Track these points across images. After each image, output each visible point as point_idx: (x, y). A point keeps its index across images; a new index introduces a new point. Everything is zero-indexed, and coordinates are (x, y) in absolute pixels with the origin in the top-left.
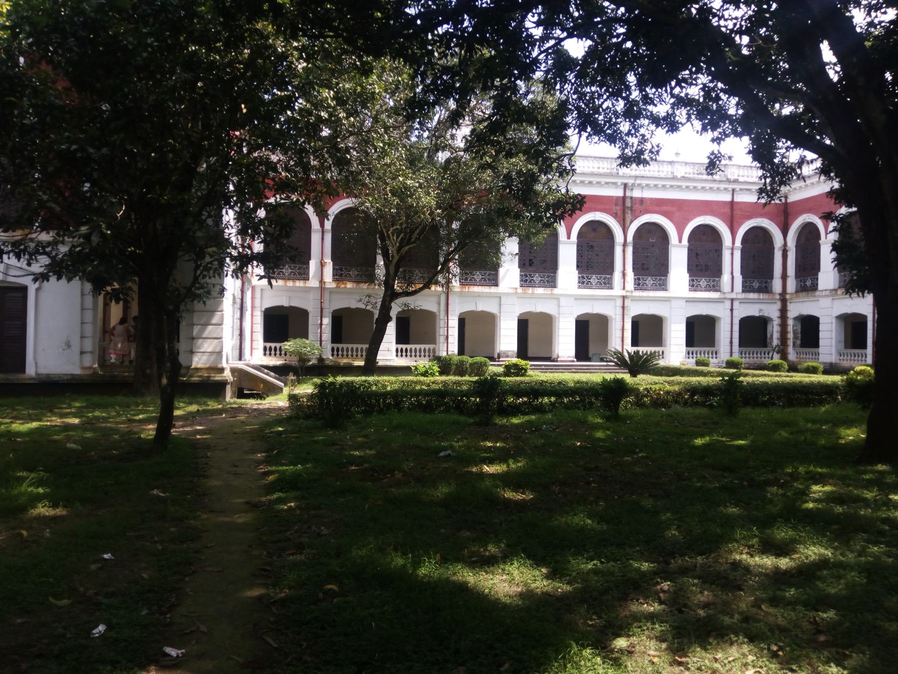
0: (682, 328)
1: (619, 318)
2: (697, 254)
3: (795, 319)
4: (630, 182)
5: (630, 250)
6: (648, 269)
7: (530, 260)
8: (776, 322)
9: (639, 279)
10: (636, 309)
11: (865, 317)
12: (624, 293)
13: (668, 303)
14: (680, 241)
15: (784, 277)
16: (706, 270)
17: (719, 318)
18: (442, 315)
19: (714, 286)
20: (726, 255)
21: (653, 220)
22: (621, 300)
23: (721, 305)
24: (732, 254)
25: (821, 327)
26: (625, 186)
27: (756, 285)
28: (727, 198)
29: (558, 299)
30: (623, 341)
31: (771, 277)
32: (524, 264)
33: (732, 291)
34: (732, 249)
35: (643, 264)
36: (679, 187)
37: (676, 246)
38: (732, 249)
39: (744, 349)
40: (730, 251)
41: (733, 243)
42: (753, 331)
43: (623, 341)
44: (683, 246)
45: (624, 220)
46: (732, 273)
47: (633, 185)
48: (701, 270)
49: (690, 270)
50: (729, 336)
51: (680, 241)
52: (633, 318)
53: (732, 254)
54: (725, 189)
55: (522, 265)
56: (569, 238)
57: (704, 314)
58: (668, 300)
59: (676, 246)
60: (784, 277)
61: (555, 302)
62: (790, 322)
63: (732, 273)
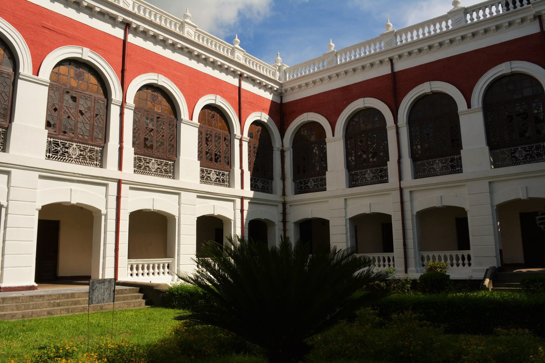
2: (207, 140)
3: (296, 223)
4: (135, 23)
6: (151, 147)
8: (279, 227)
9: (140, 160)
10: (134, 201)
11: (389, 217)
15: (283, 178)
16: (216, 161)
21: (160, 83)
22: (116, 184)
25: (332, 230)
27: (260, 184)
29: (8, 173)
31: (271, 178)
34: (241, 140)
35: (146, 139)
45: (123, 71)
48: (211, 160)
49: (200, 158)
53: (241, 145)
56: (36, 72)
58: (176, 192)
60: (283, 178)
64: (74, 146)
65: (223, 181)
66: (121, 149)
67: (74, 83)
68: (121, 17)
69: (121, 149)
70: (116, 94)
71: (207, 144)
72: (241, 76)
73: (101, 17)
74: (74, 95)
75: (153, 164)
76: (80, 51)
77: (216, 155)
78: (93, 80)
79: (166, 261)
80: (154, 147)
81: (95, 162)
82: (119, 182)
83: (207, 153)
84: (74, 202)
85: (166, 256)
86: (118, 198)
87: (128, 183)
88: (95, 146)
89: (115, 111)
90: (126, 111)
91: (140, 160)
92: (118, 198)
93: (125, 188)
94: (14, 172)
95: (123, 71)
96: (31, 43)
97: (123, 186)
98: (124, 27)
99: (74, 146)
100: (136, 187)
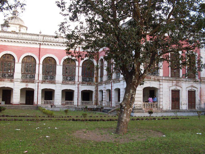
0: (60, 94)
1: (37, 90)
4: (42, 43)
20: (77, 68)
22: (38, 83)
30: (38, 98)
33: (78, 81)
36: (60, 45)
39: (83, 102)
41: (79, 65)
42: (86, 95)
43: (38, 98)
45: (39, 56)
52: (43, 90)
62: (99, 92)
85: (52, 100)
89: (37, 66)
92: (38, 86)
95: (39, 56)
96: (17, 55)
97: (39, 83)
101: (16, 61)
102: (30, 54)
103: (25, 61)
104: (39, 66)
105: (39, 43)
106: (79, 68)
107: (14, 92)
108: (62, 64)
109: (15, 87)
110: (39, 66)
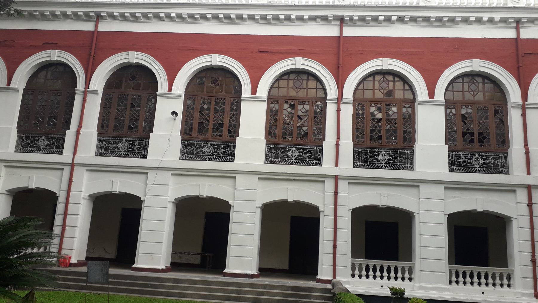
0: (442, 230)
4: (347, 14)
5: (347, 111)
7: (200, 124)
10: (356, 197)
12: (335, 171)
13: (414, 191)
14: (431, 95)
17: (511, 218)
18: (62, 199)
19: (495, 165)
21: (385, 67)
23: (510, 196)
24: (524, 115)
26: (342, 20)
28: (509, 33)
30: (335, 247)
32: (191, 130)
34: (523, 108)
35: (372, 131)
37: (423, 103)
38: (523, 108)
40: (519, 112)
43: (335, 247)
44: (438, 104)
46: (526, 145)
47: (351, 19)
50: (529, 249)
51: (431, 95)
53: (524, 115)
54: (504, 21)
55: (187, 132)
56: (254, 92)
57: (480, 209)
59: (423, 103)
61: (230, 181)
63: (526, 145)
64: (294, 149)
65: (495, 165)
66: (337, 145)
67: (292, 93)
68: (331, 14)
69: (337, 145)
70: (332, 93)
71: (463, 122)
72: (518, 22)
73: (313, 23)
74: (292, 103)
75: (383, 156)
76: (293, 62)
77: (480, 134)
78: (312, 84)
79: (406, 264)
80: (384, 138)
81: (315, 161)
82: (336, 178)
83: (464, 134)
84: (290, 199)
86: (336, 194)
87: (345, 178)
88: (314, 146)
89: (331, 109)
90: (342, 106)
91: (366, 153)
92: (336, 194)
93: (343, 185)
94: (238, 176)
98: (338, 23)
99: (294, 149)
100: (354, 181)
101: (246, 92)
102: (299, 63)
103: (283, 92)
104: (339, 110)
105: (336, 18)
106: (528, 112)
107: (234, 217)
108: (440, 95)
109: (238, 194)
110: (339, 110)
